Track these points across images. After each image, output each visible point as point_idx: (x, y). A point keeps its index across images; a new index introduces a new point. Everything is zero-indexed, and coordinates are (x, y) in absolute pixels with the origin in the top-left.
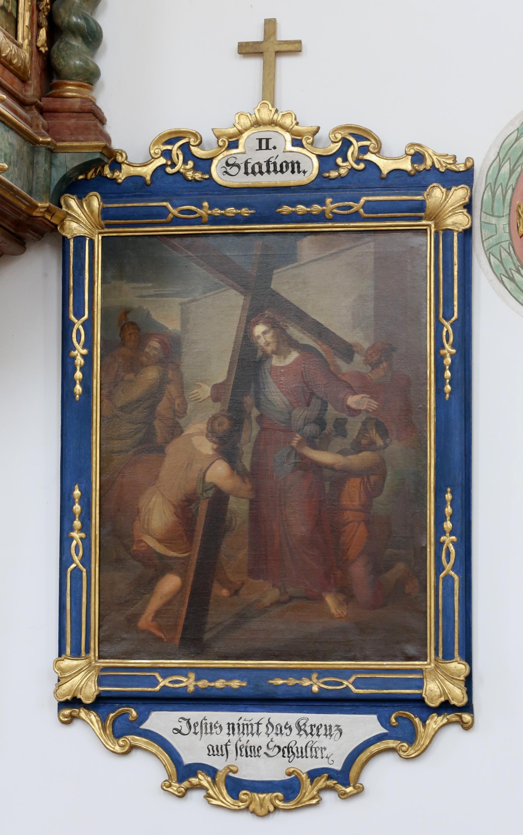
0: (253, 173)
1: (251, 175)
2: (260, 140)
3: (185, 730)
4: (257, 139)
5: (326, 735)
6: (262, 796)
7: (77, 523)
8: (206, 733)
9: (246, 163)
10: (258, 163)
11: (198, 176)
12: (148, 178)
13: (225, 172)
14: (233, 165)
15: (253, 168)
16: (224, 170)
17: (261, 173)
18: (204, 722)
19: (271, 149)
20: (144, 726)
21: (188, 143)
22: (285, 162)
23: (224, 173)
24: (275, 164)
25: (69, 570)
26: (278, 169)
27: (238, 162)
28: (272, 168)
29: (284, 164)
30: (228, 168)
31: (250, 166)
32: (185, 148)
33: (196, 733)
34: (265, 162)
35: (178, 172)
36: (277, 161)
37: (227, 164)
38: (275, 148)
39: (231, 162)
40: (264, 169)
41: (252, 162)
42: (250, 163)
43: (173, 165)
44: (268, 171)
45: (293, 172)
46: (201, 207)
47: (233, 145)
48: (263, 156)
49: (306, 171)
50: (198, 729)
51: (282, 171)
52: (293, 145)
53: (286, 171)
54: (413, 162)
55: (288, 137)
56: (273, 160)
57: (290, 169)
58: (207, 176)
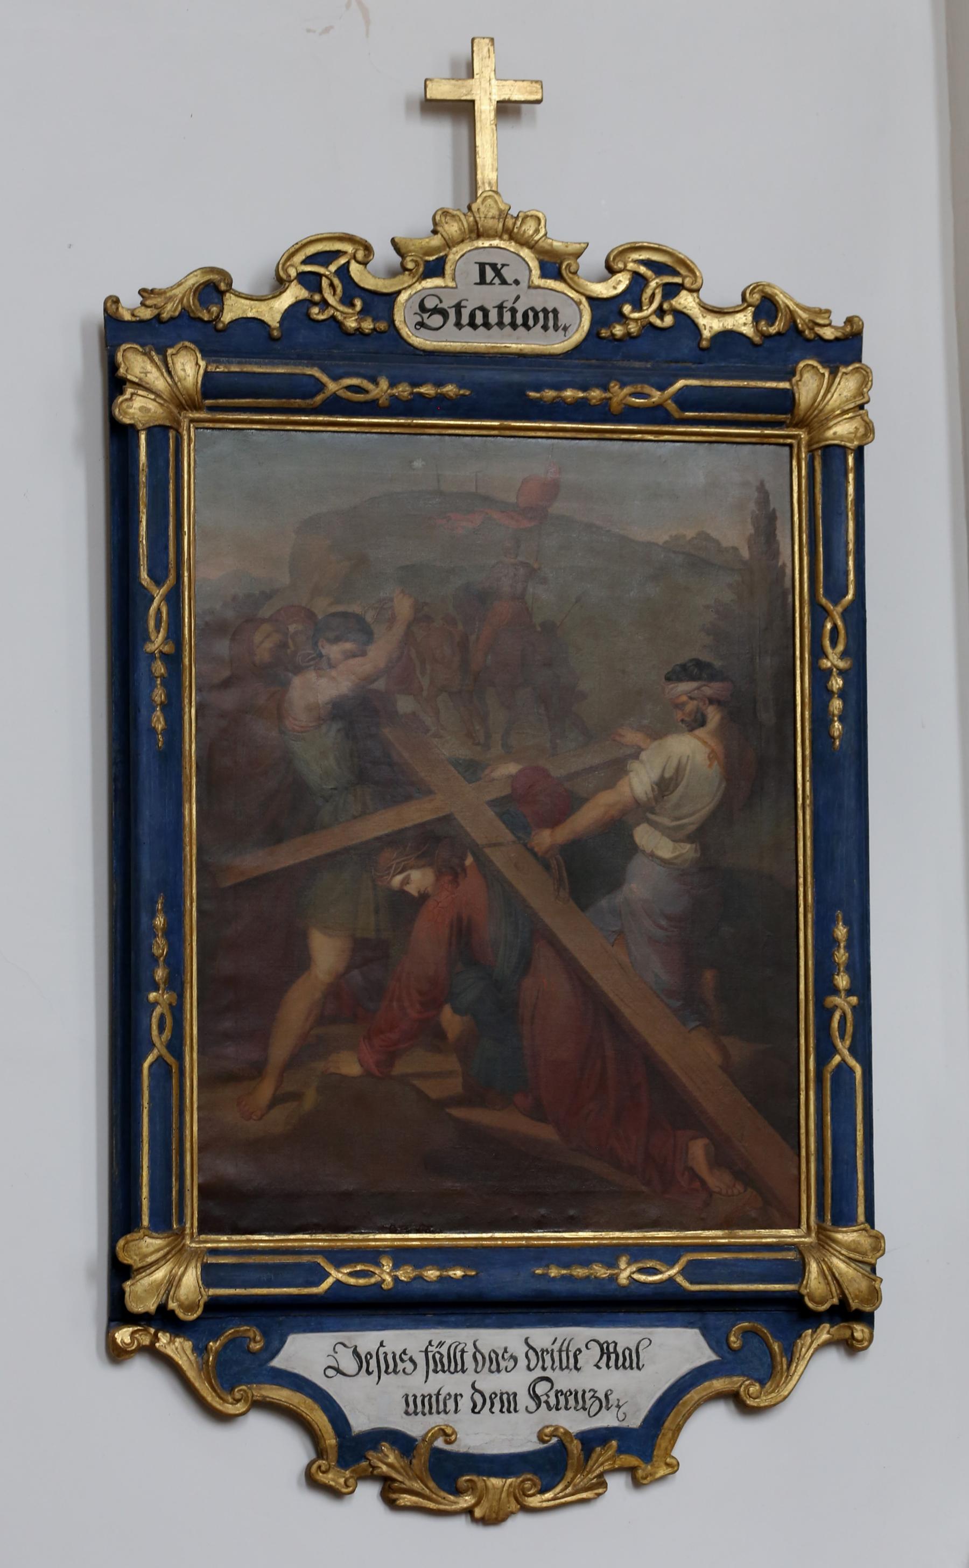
0: (472, 324)
2: (482, 266)
4: (476, 263)
5: (561, 1368)
8: (436, 1371)
9: (458, 307)
10: (482, 308)
13: (418, 324)
14: (436, 311)
15: (472, 316)
16: (419, 319)
17: (487, 325)
18: (382, 1350)
21: (346, 266)
22: (532, 309)
23: (418, 327)
24: (513, 311)
25: (146, 1065)
26: (519, 320)
27: (444, 305)
28: (507, 318)
29: (531, 314)
30: (426, 316)
32: (344, 272)
33: (369, 1373)
34: (494, 307)
36: (516, 305)
39: (430, 303)
40: (493, 318)
42: (466, 307)
44: (500, 324)
46: (376, 383)
48: (492, 295)
49: (567, 325)
51: (525, 325)
52: (544, 275)
53: (534, 326)
56: (508, 305)
58: (382, 326)
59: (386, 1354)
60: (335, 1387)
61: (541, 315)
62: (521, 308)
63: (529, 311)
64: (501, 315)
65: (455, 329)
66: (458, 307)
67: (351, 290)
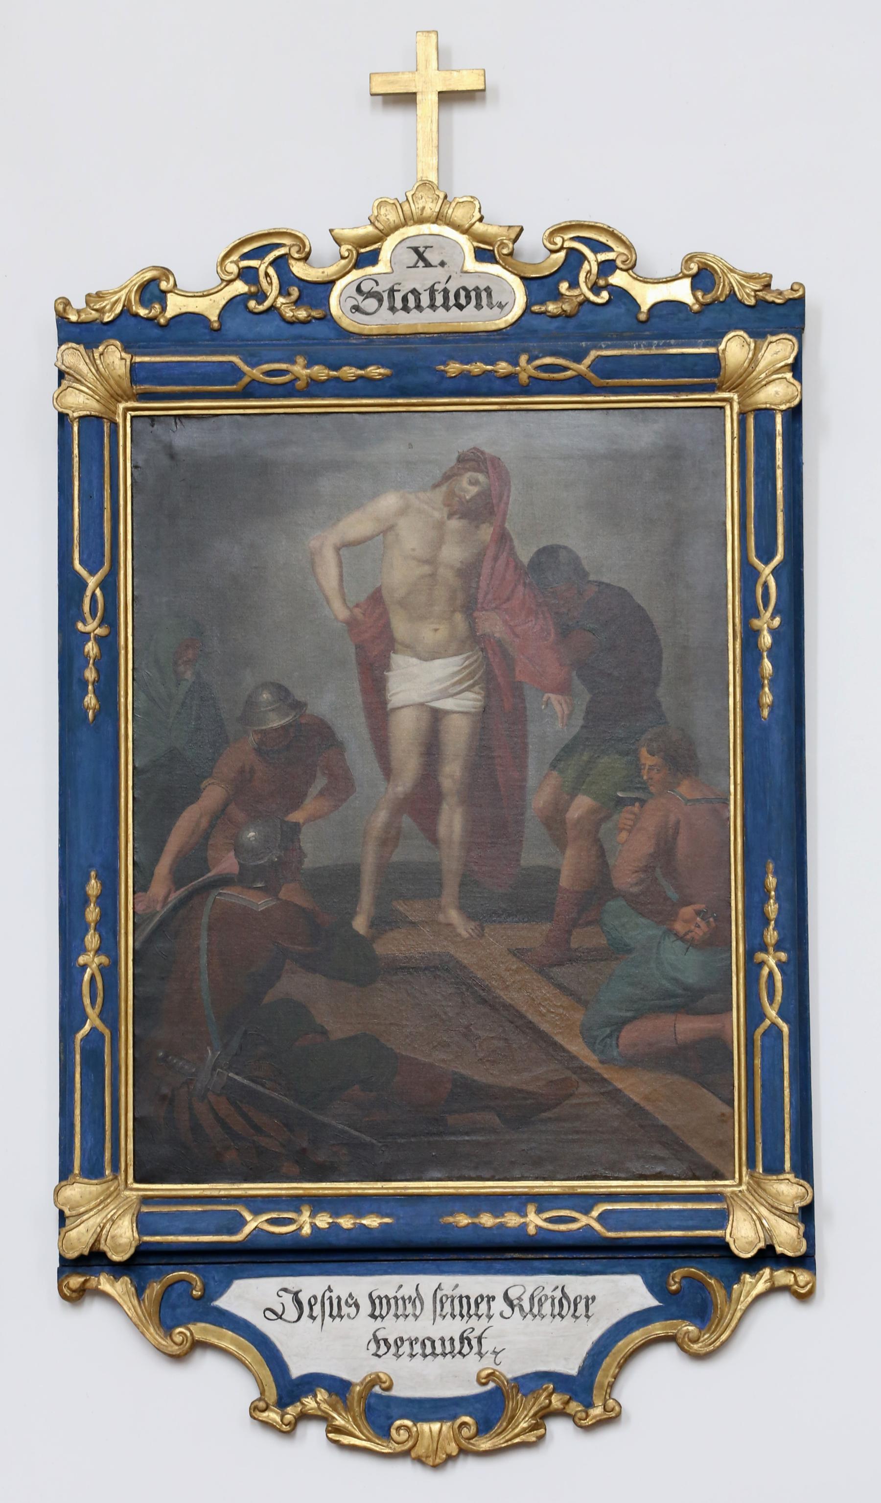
0: (406, 308)
6: (436, 1426)
7: (92, 940)
9: (392, 291)
10: (414, 291)
12: (214, 317)
14: (370, 294)
15: (405, 299)
18: (327, 1295)
19: (436, 266)
22: (464, 288)
23: (354, 311)
24: (446, 291)
28: (439, 300)
29: (462, 293)
31: (398, 296)
32: (280, 264)
33: (312, 1318)
35: (272, 308)
36: (448, 286)
38: (442, 264)
40: (425, 300)
41: (406, 288)
43: (261, 296)
44: (432, 306)
45: (479, 306)
48: (421, 279)
50: (317, 1309)
54: (694, 288)
55: (466, 245)
57: (473, 302)
59: (330, 1298)
60: (272, 1329)
61: (473, 294)
62: (452, 287)
63: (461, 290)
64: (432, 298)
65: (390, 312)
66: (392, 291)
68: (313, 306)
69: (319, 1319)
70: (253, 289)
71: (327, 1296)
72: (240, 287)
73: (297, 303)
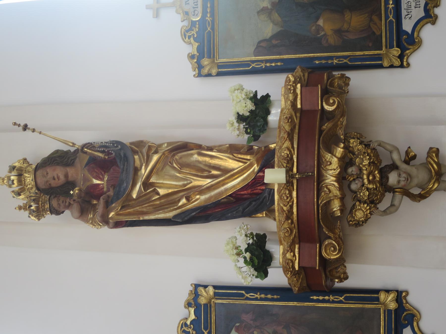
0: (197, 5)
1: (198, 6)
2: (186, 4)
3: (410, 16)
9: (194, 8)
10: (194, 3)
11: (197, 26)
14: (194, 12)
15: (195, 5)
18: (406, 9)
20: (410, 32)
23: (197, 16)
27: (193, 10)
32: (187, 31)
33: (411, 12)
37: (194, 15)
43: (193, 35)
47: (187, 13)
50: (409, 11)
59: (407, 8)
67: (191, 29)
68: (196, 24)
69: (411, 10)
70: (192, 36)
71: (406, 9)
72: (192, 39)
73: (195, 27)
